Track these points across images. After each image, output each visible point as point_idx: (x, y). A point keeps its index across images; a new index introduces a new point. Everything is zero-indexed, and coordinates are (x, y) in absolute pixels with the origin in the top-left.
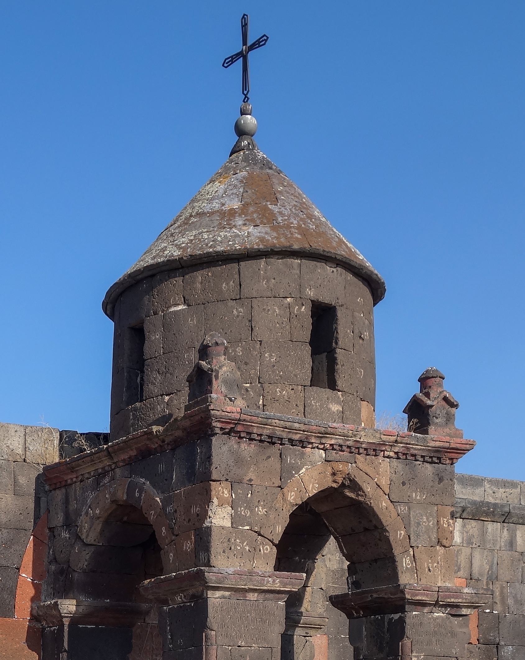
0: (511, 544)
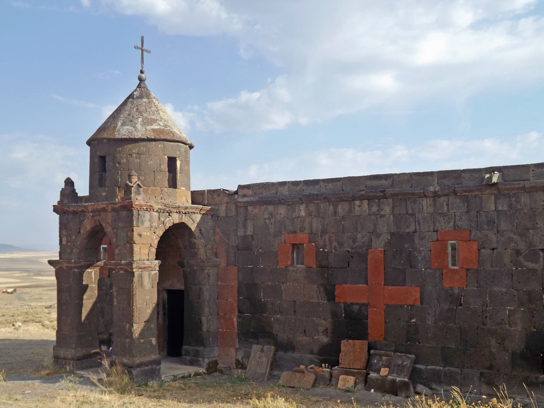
0: (335, 213)
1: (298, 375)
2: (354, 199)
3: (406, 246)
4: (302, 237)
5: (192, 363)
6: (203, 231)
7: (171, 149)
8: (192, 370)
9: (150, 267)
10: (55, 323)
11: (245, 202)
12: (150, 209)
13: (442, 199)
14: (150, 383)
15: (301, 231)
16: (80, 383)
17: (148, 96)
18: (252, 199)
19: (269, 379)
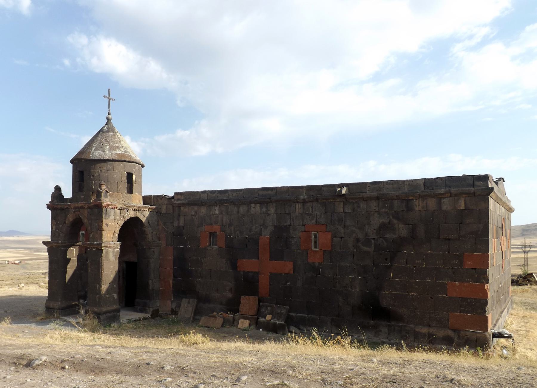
0: (238, 212)
1: (212, 319)
2: (251, 203)
3: (284, 234)
4: (216, 228)
5: (141, 311)
6: (150, 223)
7: (129, 168)
8: (141, 315)
9: (114, 246)
10: (47, 285)
11: (179, 204)
12: (114, 207)
13: (309, 204)
14: (112, 325)
15: (215, 224)
16: (64, 325)
17: (113, 130)
18: (183, 202)
19: (193, 322)
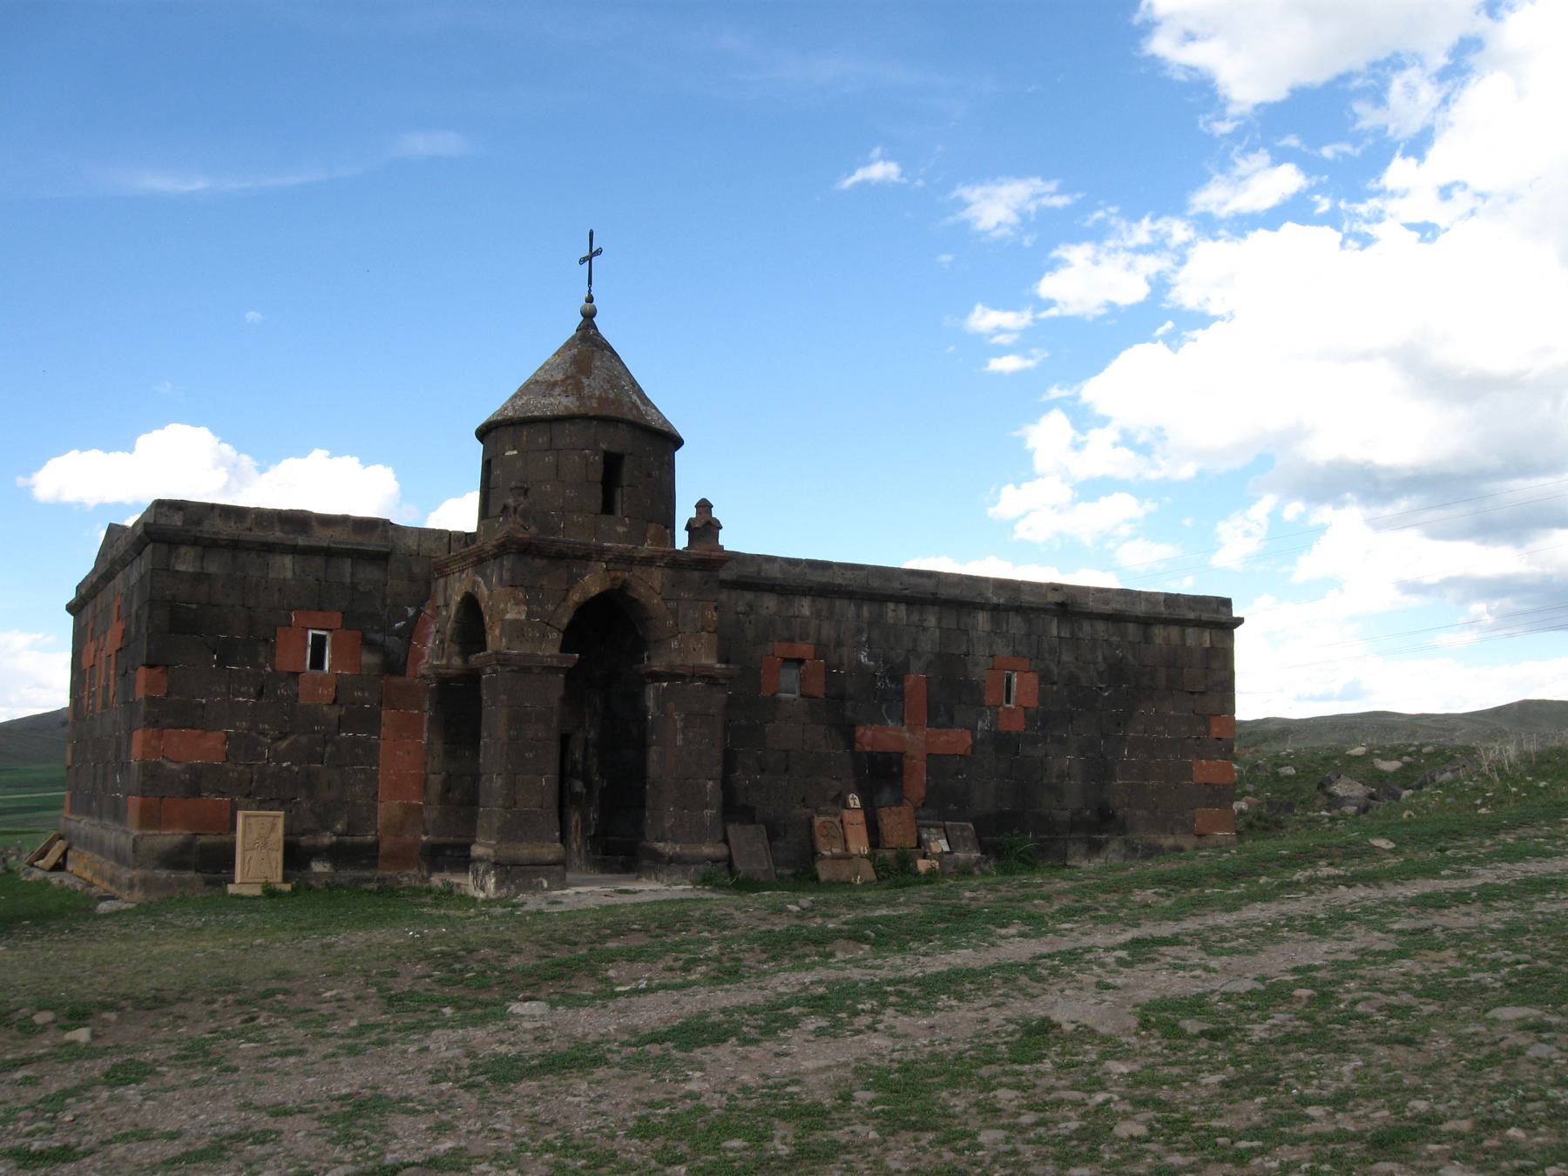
4: (804, 649)
15: (801, 639)
